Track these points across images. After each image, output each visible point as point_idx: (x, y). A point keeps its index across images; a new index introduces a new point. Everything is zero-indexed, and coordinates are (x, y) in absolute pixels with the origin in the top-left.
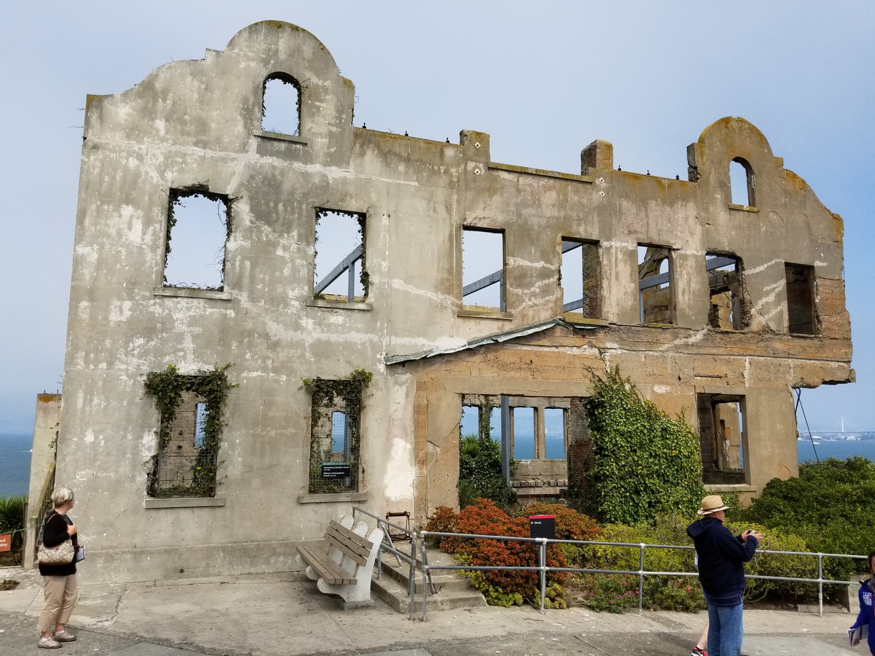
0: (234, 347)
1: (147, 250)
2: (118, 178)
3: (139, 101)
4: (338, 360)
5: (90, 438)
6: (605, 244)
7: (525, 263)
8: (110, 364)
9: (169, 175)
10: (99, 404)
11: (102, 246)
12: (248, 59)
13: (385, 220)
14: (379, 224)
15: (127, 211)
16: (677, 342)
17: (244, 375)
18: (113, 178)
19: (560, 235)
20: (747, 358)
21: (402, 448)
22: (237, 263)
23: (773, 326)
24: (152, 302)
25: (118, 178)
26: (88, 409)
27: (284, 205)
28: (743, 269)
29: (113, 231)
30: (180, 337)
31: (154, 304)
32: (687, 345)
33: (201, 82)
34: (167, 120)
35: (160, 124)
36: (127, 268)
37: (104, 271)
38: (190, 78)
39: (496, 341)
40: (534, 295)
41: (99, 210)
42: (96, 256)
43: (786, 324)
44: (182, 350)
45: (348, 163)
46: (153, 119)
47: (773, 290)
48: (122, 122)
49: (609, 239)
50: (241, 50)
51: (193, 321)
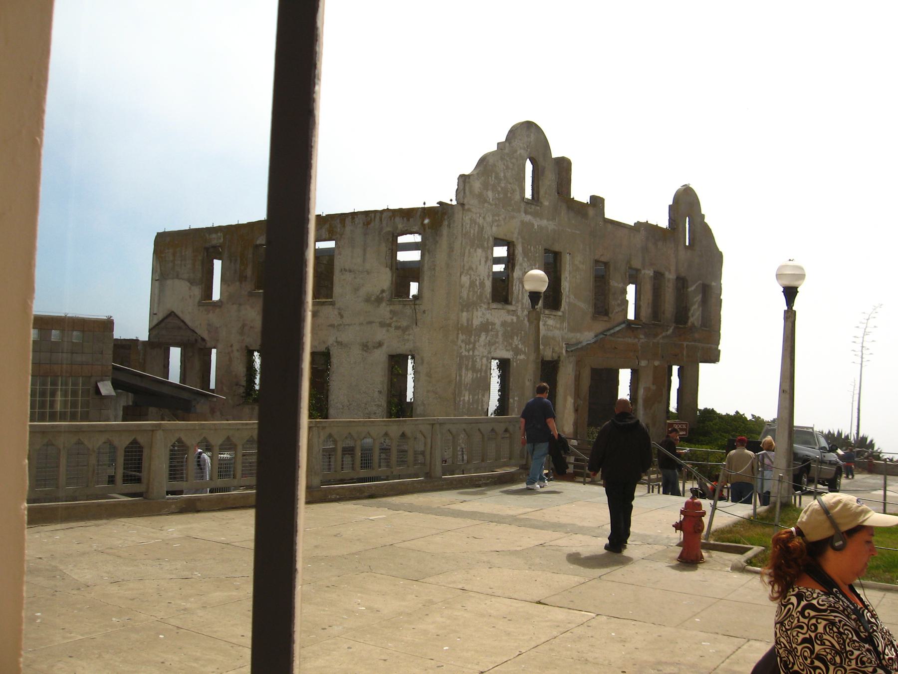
0: (515, 341)
1: (486, 279)
2: (476, 230)
3: (483, 178)
4: (550, 348)
5: (467, 398)
6: (643, 272)
7: (616, 284)
8: (473, 352)
9: (494, 229)
10: (470, 377)
11: (470, 275)
12: (521, 148)
13: (568, 256)
14: (566, 259)
15: (479, 251)
16: (664, 334)
17: (518, 357)
18: (474, 230)
19: (628, 265)
20: (685, 344)
21: (570, 401)
22: (517, 285)
23: (696, 324)
24: (488, 312)
25: (476, 230)
26: (466, 380)
27: (534, 248)
28: (687, 288)
29: (474, 267)
30: (497, 335)
31: (489, 313)
32: (667, 336)
33: (504, 164)
34: (493, 192)
35: (490, 194)
36: (479, 290)
37: (471, 293)
38: (500, 161)
39: (606, 335)
40: (619, 305)
41: (469, 252)
42: (468, 283)
43: (700, 323)
44: (498, 342)
45: (555, 220)
46: (487, 191)
47: (697, 301)
48: (477, 193)
49: (644, 269)
50: (518, 142)
51: (504, 324)
